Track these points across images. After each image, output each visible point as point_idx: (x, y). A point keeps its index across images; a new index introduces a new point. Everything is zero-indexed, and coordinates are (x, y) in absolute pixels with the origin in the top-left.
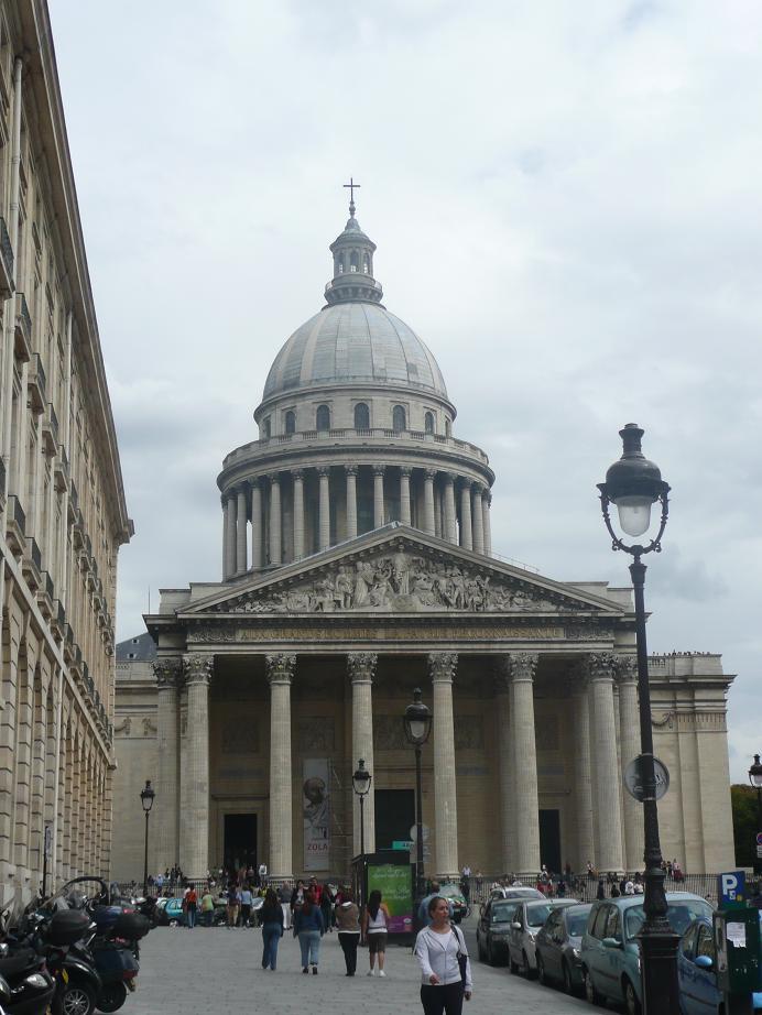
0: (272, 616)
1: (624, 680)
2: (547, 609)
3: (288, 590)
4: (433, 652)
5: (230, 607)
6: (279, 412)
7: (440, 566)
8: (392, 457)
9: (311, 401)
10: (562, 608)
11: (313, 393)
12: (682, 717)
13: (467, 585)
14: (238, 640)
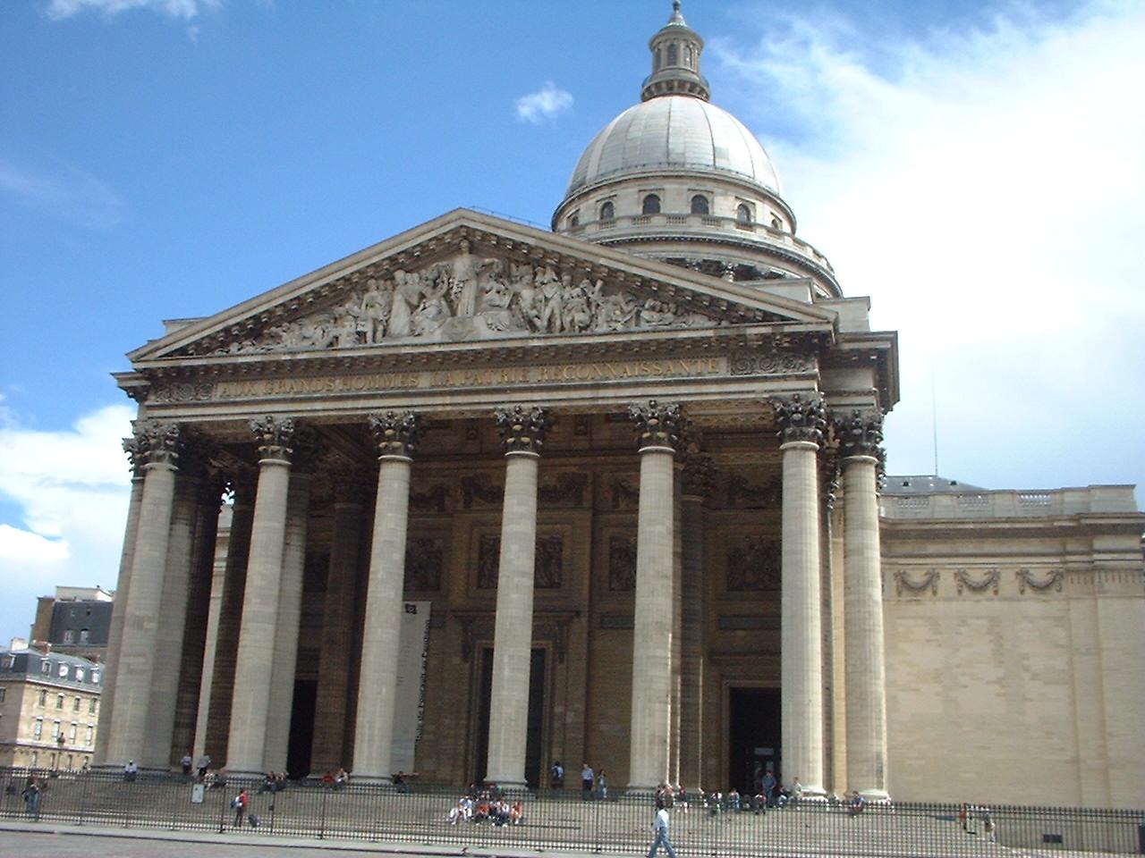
0: (259, 359)
1: (852, 451)
2: (700, 327)
3: (290, 323)
4: (500, 407)
5: (208, 350)
6: (565, 220)
7: (524, 269)
8: (674, 247)
9: (595, 200)
10: (724, 323)
11: (595, 190)
13: (566, 296)
14: (214, 399)
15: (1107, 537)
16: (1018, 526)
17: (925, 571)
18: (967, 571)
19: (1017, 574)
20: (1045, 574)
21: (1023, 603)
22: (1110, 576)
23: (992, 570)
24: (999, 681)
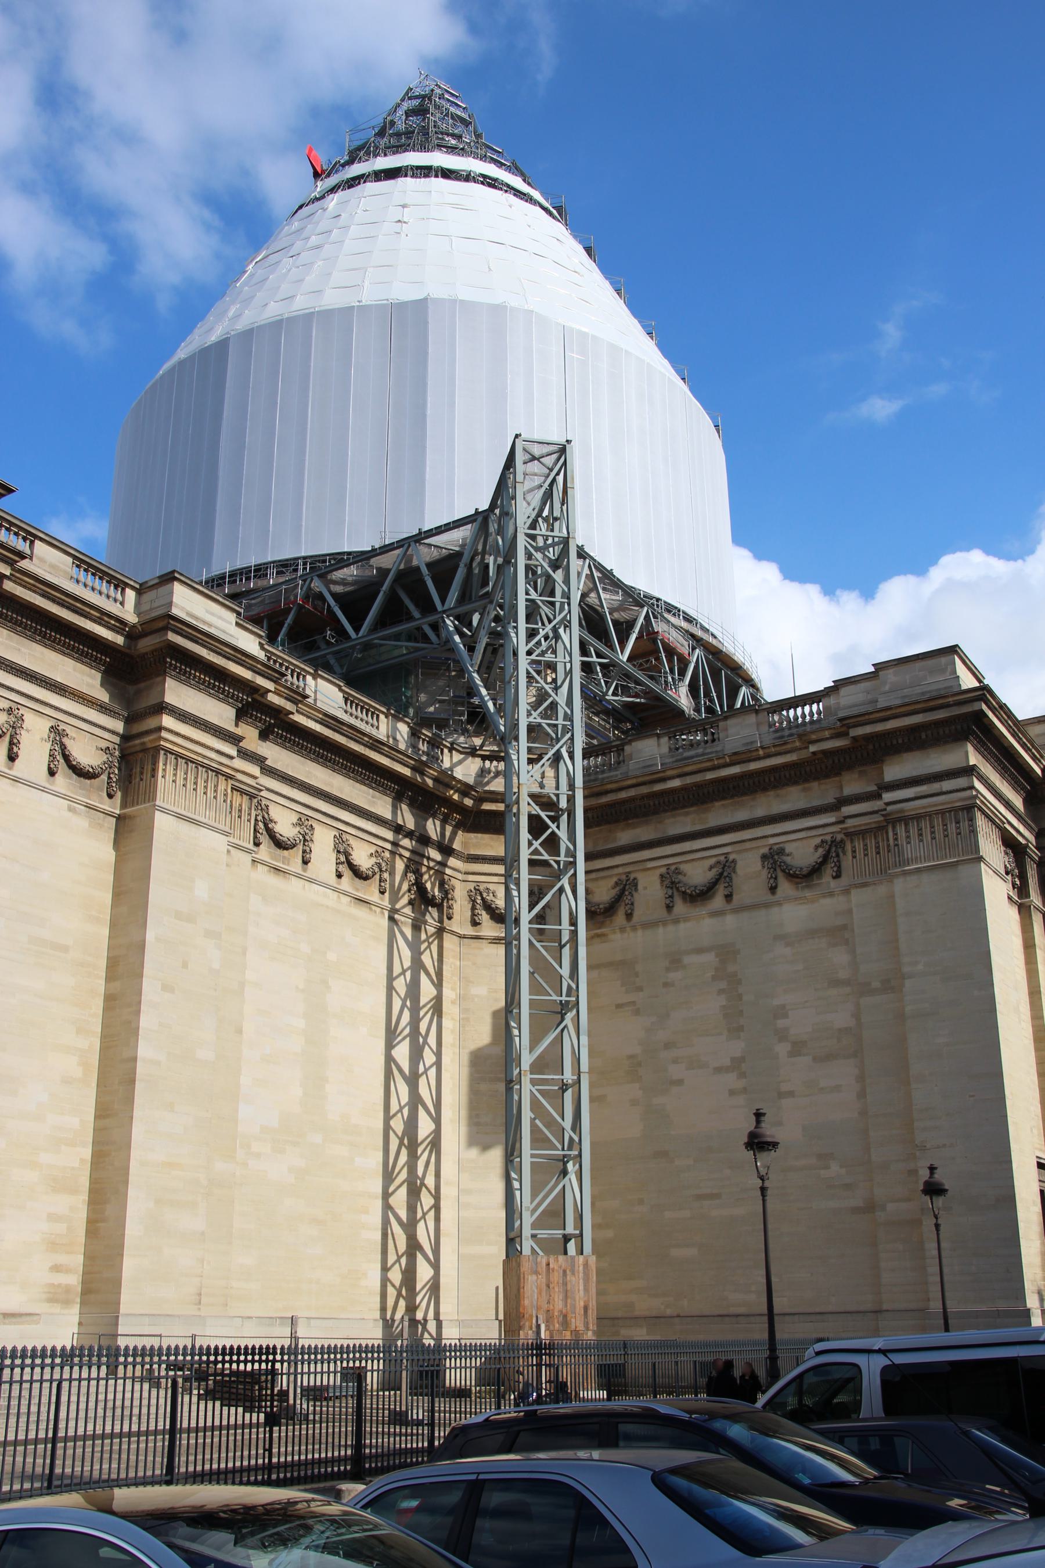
12: (859, 845)
15: (907, 756)
16: (753, 766)
17: (615, 879)
18: (682, 867)
19: (764, 857)
20: (812, 850)
21: (775, 910)
22: (913, 831)
23: (722, 858)
24: (737, 1064)
